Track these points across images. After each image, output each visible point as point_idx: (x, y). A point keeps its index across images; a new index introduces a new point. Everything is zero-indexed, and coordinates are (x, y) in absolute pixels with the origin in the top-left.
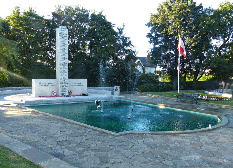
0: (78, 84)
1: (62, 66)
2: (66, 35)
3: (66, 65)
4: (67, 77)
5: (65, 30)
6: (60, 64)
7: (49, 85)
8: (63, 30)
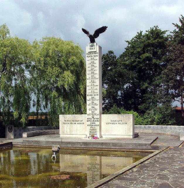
0: (118, 122)
1: (90, 97)
3: (96, 95)
4: (98, 112)
7: (77, 122)
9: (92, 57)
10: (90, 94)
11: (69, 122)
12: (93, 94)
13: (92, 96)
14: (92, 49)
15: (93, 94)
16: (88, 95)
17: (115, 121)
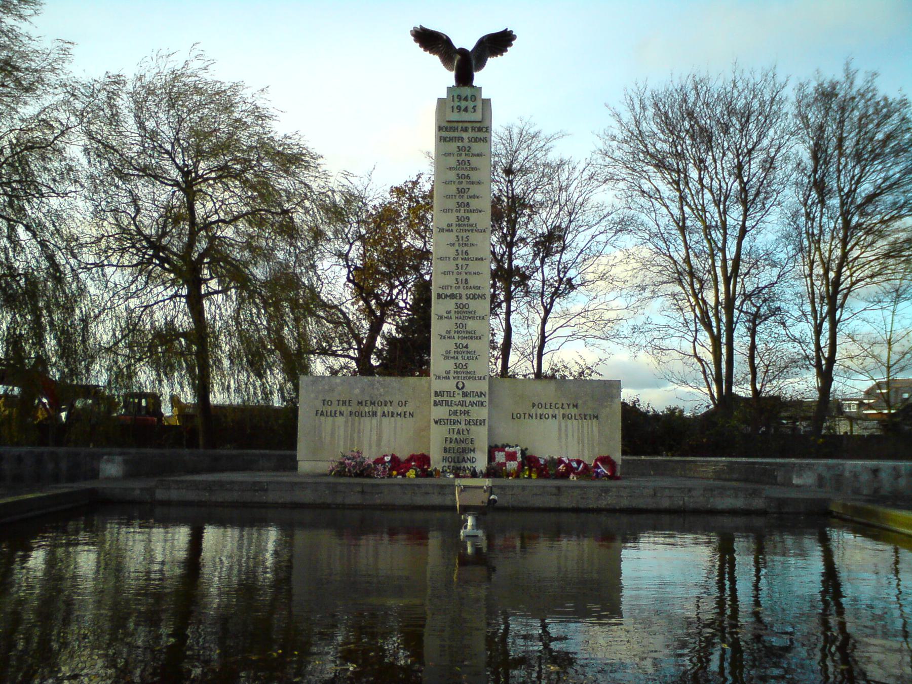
1: (451, 304)
2: (480, 130)
3: (474, 297)
5: (470, 104)
6: (441, 291)
8: (463, 104)
9: (460, 144)
10: (449, 292)
11: (343, 408)
12: (461, 291)
13: (459, 301)
14: (466, 110)
15: (464, 292)
16: (439, 296)
17: (548, 406)
